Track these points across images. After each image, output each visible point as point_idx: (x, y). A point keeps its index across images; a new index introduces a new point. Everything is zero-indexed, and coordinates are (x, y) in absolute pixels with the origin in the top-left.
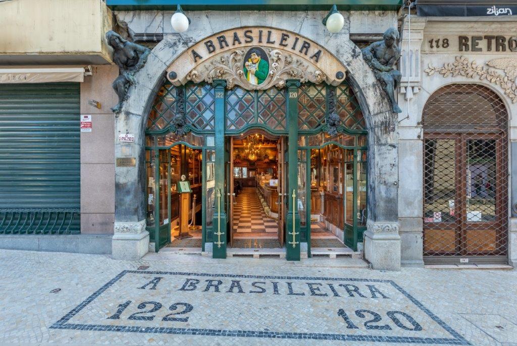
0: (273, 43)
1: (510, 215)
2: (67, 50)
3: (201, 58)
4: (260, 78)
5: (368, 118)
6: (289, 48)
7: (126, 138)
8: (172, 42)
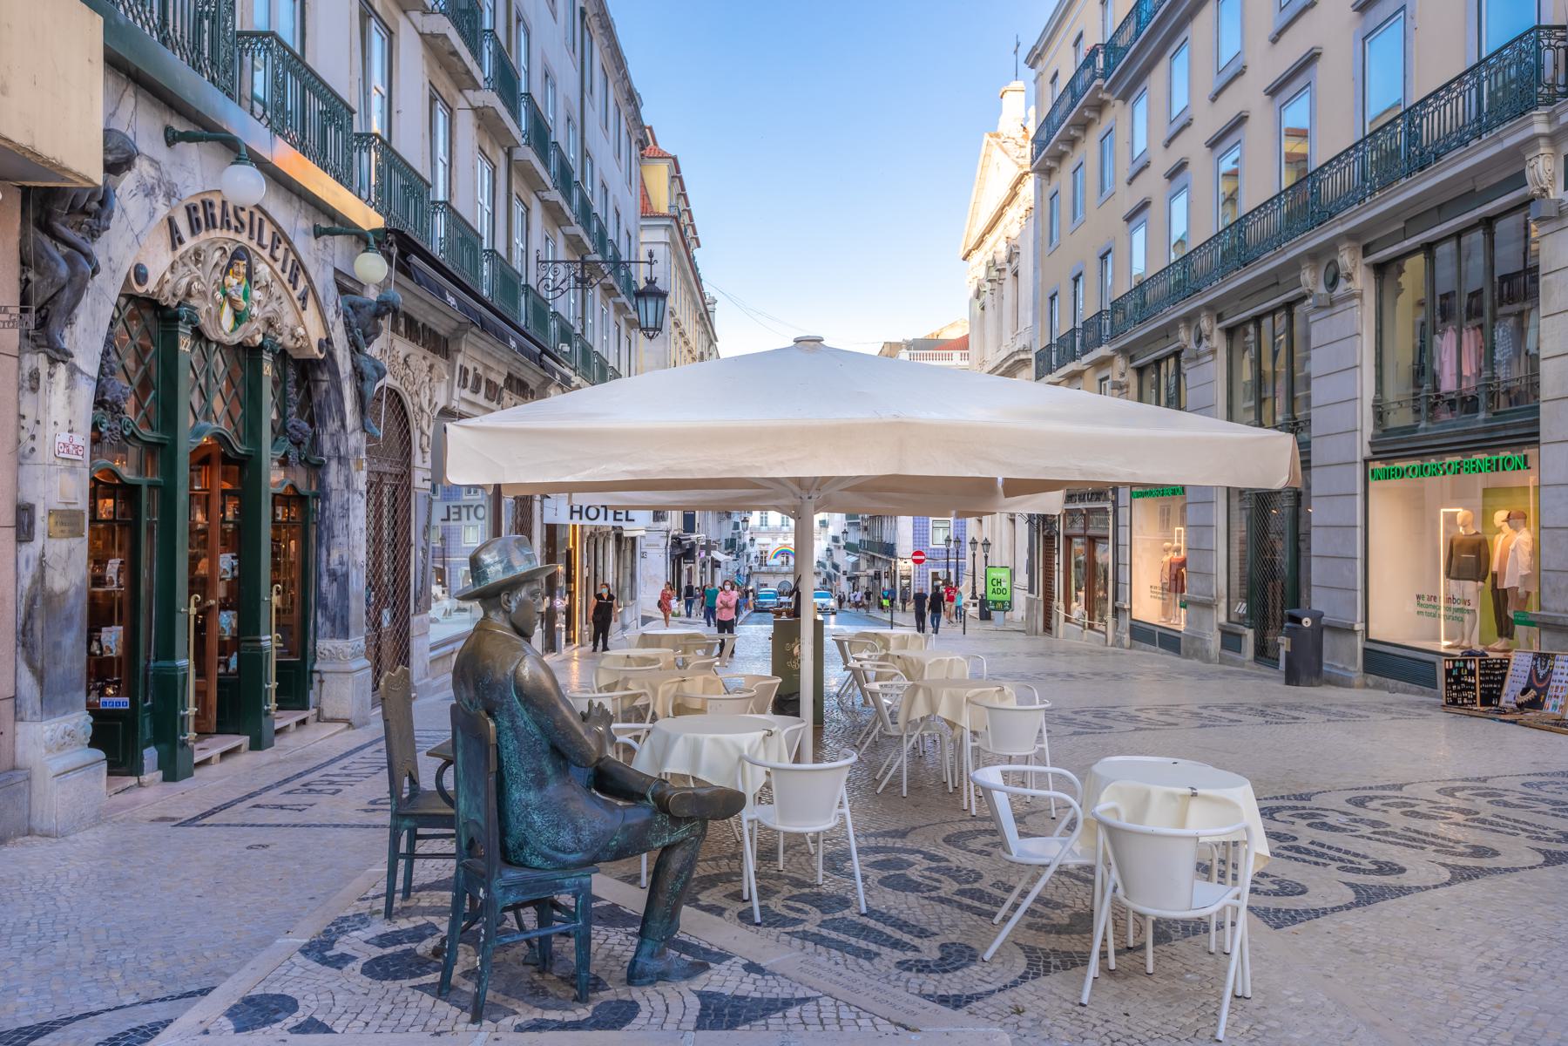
0: (264, 247)
1: (412, 611)
2: (39, 149)
3: (181, 241)
4: (239, 318)
5: (332, 435)
6: (278, 267)
7: (71, 447)
8: (150, 181)
